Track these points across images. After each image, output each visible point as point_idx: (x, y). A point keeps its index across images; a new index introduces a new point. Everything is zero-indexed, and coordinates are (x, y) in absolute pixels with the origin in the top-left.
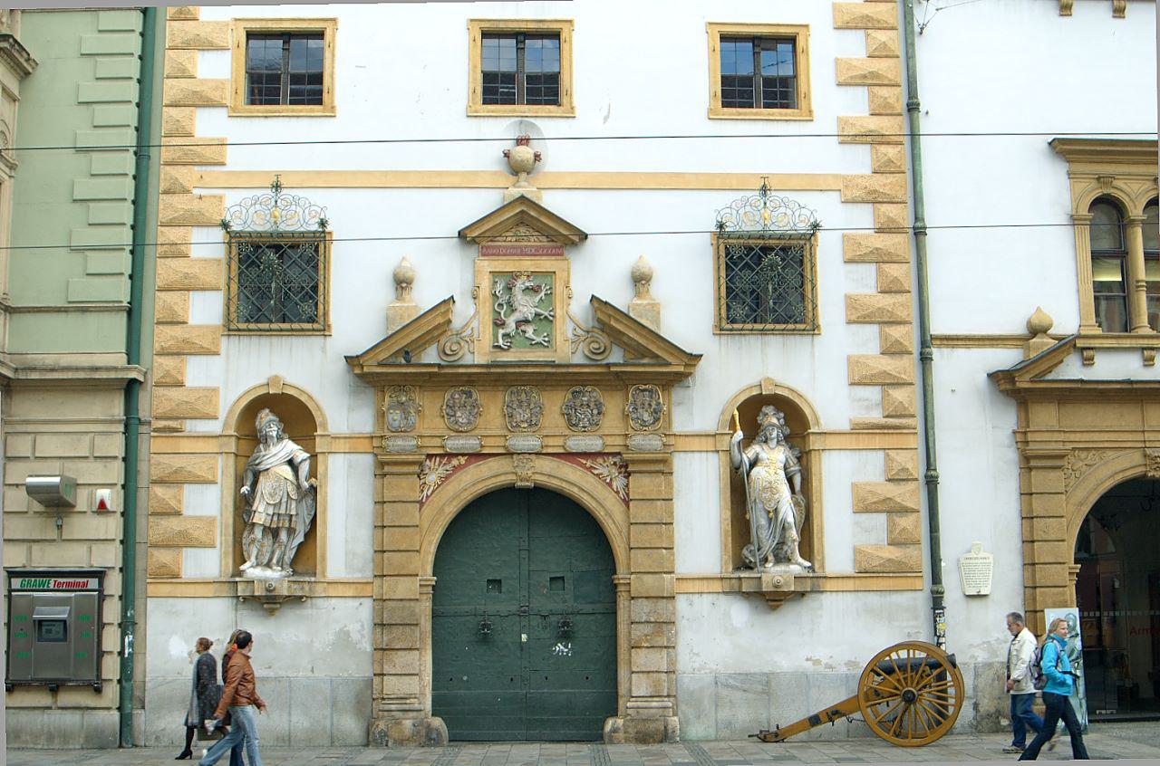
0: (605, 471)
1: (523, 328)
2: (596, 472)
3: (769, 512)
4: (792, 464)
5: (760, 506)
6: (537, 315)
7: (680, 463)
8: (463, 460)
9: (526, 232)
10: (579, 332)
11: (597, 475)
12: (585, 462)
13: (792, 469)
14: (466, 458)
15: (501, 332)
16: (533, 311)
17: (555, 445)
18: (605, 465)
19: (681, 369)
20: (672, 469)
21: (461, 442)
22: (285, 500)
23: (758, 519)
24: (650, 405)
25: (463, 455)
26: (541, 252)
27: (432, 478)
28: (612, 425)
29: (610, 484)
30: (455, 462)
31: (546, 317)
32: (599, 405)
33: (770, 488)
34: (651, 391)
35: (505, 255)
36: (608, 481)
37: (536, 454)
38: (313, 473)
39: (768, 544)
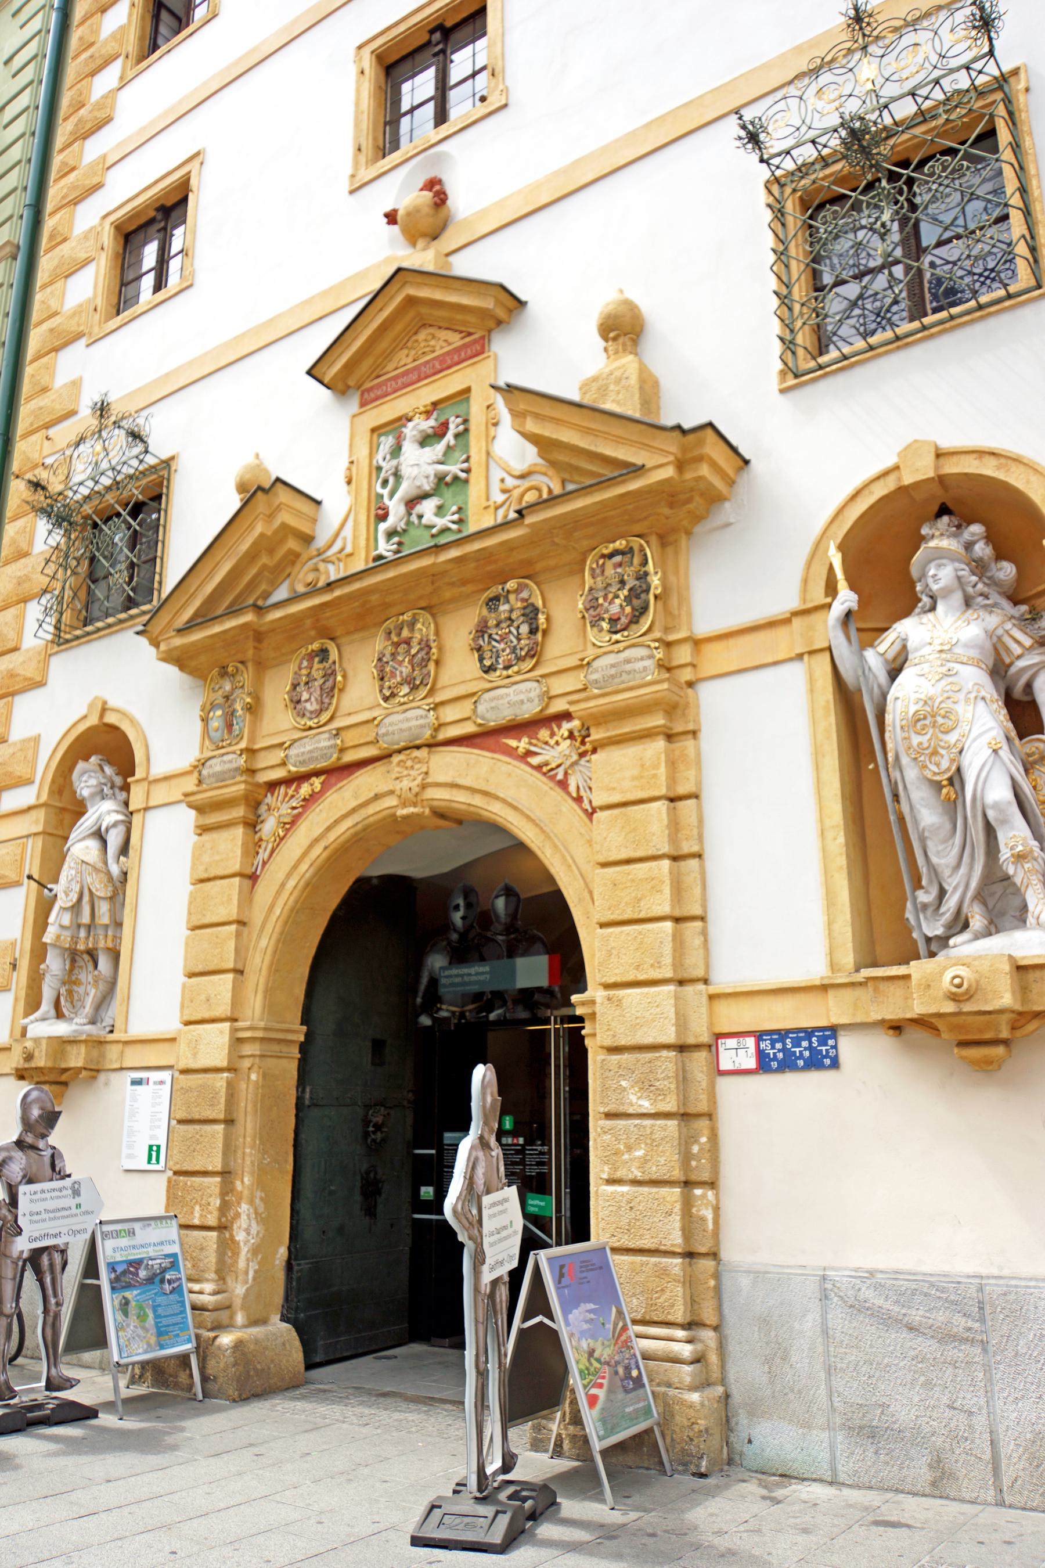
0: (549, 755)
1: (419, 509)
2: (535, 761)
3: (938, 786)
4: (1017, 650)
5: (911, 774)
6: (440, 479)
7: (718, 703)
8: (317, 782)
9: (413, 332)
10: (510, 482)
11: (538, 768)
12: (513, 743)
13: (1021, 664)
14: (323, 778)
15: (383, 527)
16: (431, 470)
17: (457, 719)
18: (552, 742)
19: (669, 472)
20: (697, 721)
21: (308, 748)
22: (86, 898)
23: (926, 813)
24: (622, 582)
25: (317, 773)
26: (449, 362)
27: (269, 826)
28: (581, 653)
29: (563, 784)
30: (305, 789)
31: (456, 478)
32: (531, 613)
33: (931, 718)
34: (628, 552)
35: (395, 391)
36: (560, 777)
37: (429, 746)
38: (124, 850)
39: (961, 882)
